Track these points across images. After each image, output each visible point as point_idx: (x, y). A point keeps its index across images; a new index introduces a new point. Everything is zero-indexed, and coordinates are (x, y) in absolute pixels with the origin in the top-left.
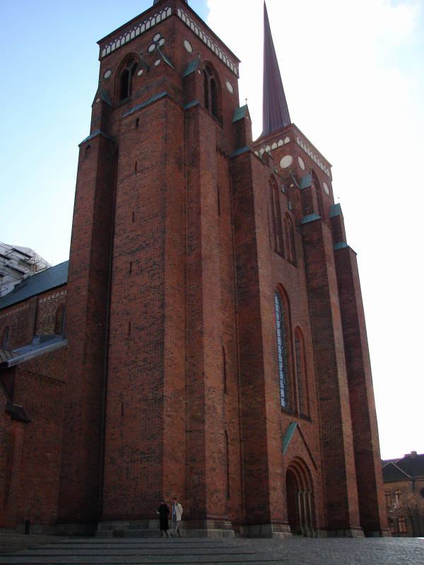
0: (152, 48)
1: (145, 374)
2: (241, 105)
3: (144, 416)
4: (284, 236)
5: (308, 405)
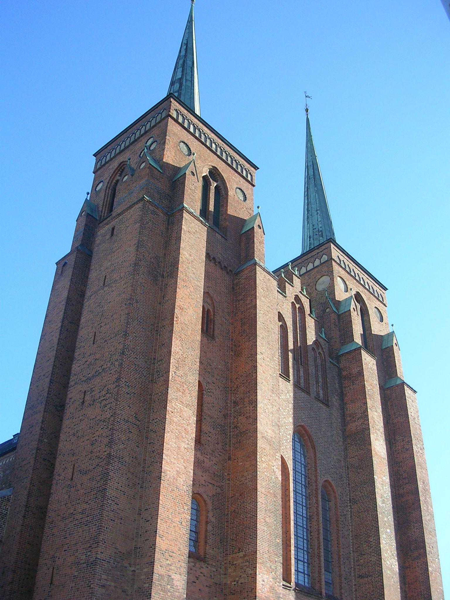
1: (80, 530)
3: (73, 585)
4: (312, 370)
5: (341, 583)
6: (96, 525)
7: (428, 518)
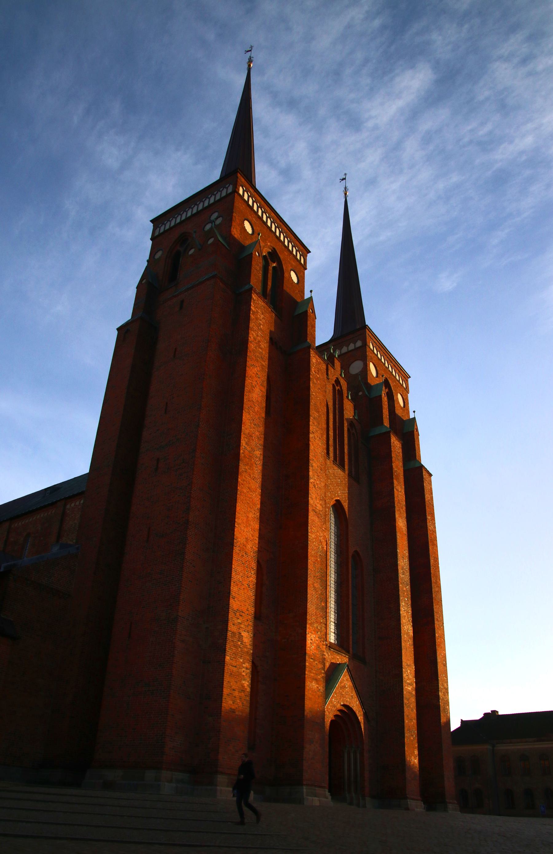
0: (208, 227)
2: (307, 295)
6: (176, 585)
7: (437, 589)
